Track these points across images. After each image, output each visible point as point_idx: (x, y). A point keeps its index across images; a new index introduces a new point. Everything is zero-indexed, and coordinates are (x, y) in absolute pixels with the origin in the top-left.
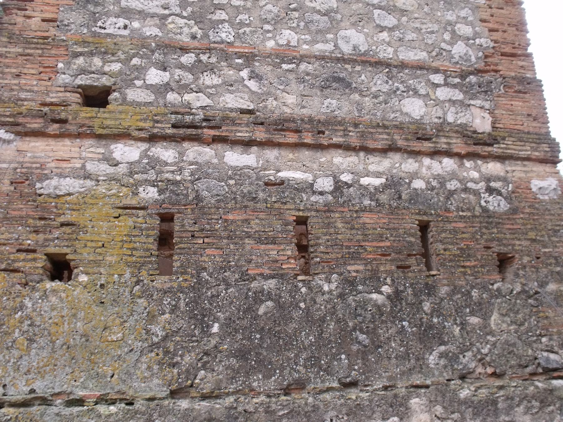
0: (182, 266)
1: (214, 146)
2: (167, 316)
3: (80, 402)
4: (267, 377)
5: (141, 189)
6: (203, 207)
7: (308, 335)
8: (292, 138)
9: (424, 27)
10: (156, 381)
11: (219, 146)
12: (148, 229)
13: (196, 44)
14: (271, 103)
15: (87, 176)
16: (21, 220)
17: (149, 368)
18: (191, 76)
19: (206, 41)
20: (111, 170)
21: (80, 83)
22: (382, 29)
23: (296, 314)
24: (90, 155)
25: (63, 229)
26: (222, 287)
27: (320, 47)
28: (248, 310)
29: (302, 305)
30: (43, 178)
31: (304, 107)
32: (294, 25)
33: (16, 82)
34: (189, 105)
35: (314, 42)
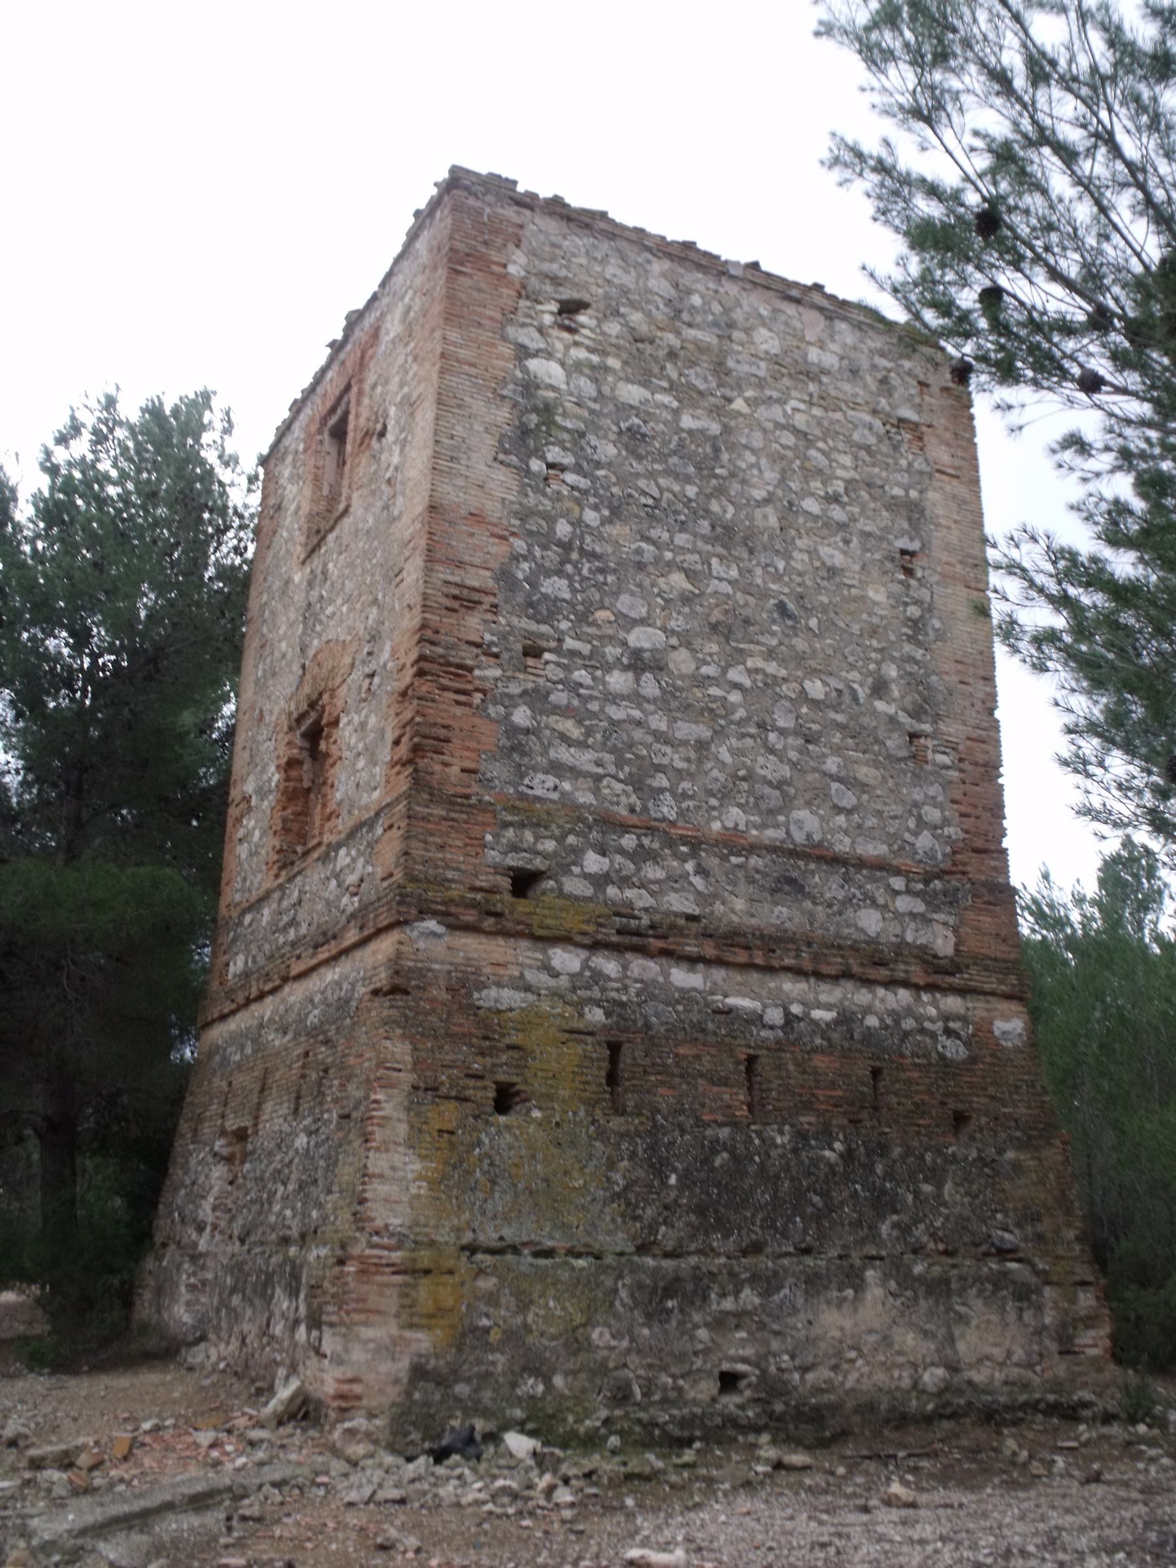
0: (636, 1106)
1: (659, 960)
2: (626, 1163)
3: (549, 1253)
4: (726, 1236)
5: (587, 1010)
6: (652, 1037)
7: (763, 1193)
8: (742, 957)
9: (887, 808)
10: (620, 1235)
11: (664, 961)
12: (598, 1060)
13: (634, 820)
14: (719, 907)
15: (528, 988)
16: (465, 1037)
17: (613, 1220)
18: (632, 866)
19: (645, 817)
20: (552, 982)
21: (512, 863)
22: (839, 810)
23: (753, 1169)
24: (527, 961)
25: (511, 1052)
26: (677, 1133)
27: (770, 833)
28: (703, 1162)
29: (757, 1159)
30: (483, 986)
31: (753, 916)
32: (743, 801)
33: (440, 855)
34: (630, 905)
35: (763, 826)
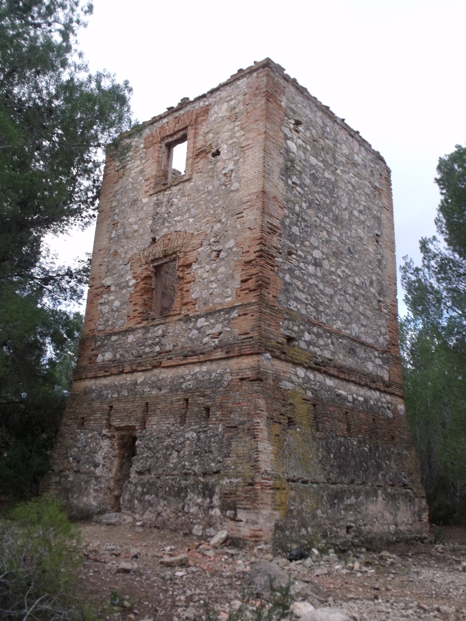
11: (324, 375)
35: (345, 329)
